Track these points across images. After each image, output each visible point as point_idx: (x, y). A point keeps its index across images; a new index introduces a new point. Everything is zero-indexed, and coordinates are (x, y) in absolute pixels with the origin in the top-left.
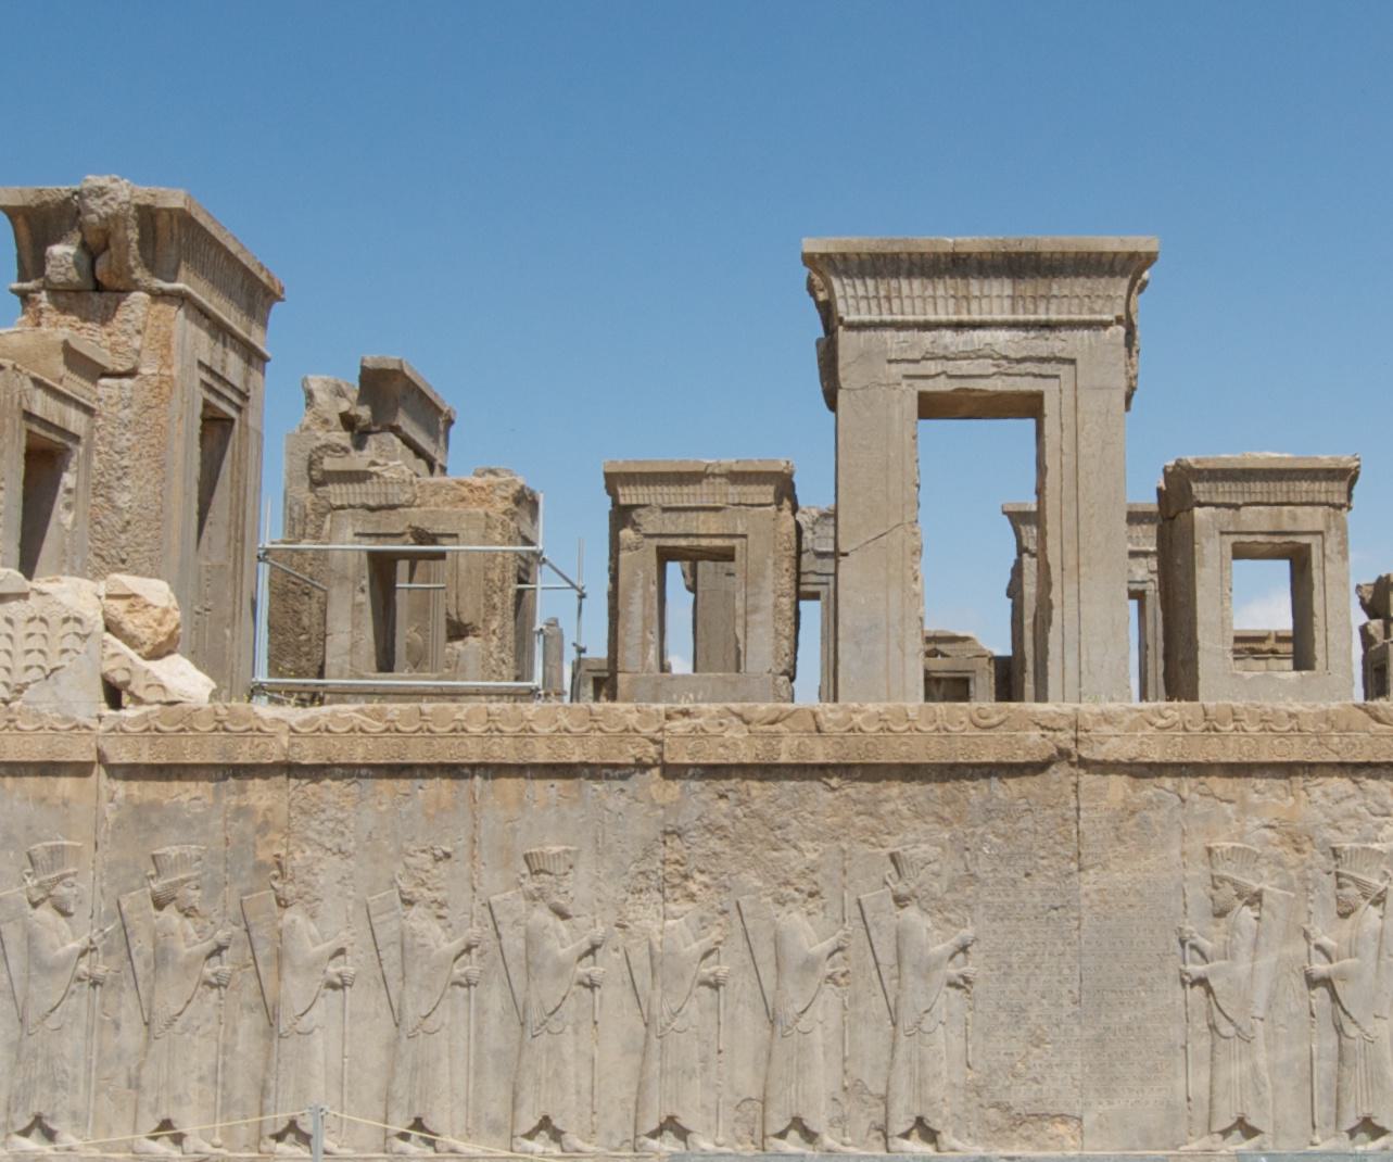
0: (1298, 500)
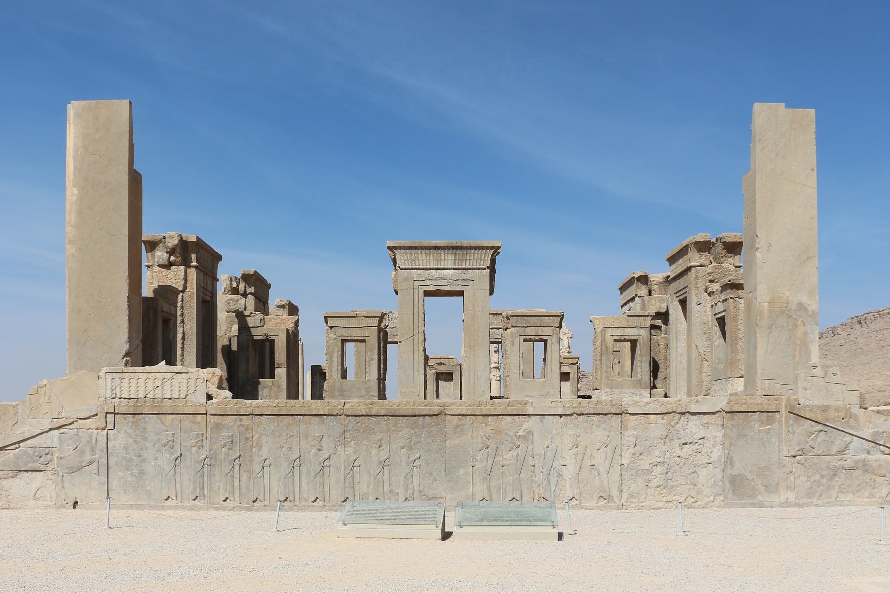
0: (545, 325)
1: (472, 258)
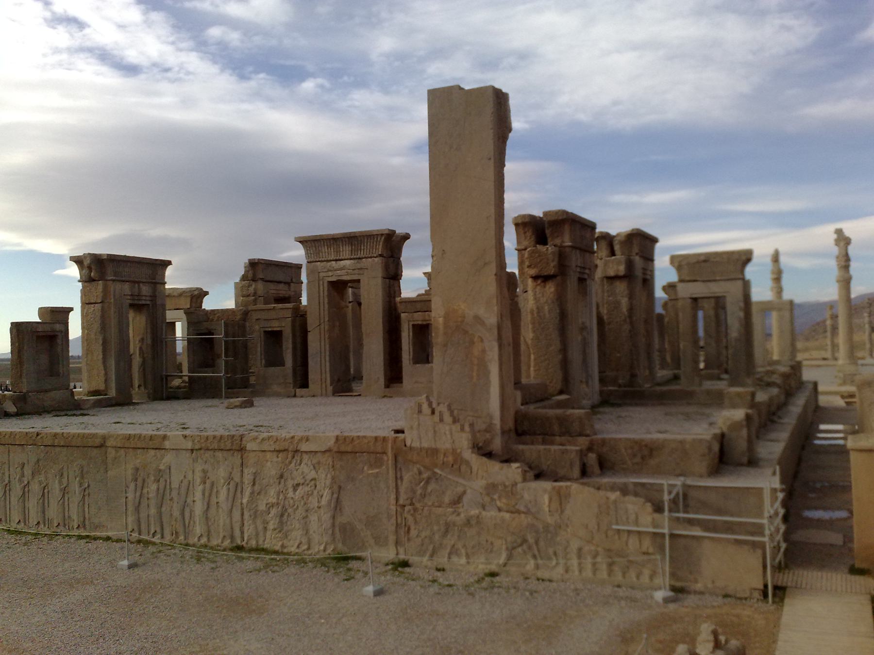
1: (365, 248)
